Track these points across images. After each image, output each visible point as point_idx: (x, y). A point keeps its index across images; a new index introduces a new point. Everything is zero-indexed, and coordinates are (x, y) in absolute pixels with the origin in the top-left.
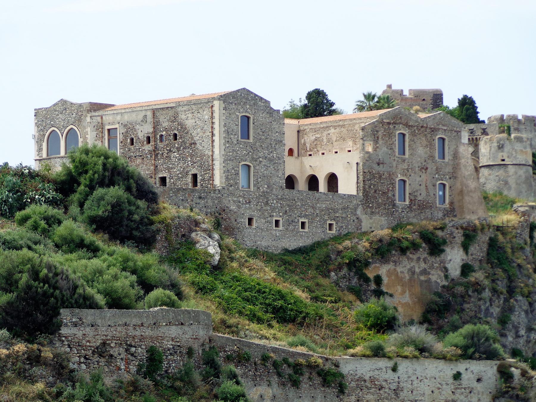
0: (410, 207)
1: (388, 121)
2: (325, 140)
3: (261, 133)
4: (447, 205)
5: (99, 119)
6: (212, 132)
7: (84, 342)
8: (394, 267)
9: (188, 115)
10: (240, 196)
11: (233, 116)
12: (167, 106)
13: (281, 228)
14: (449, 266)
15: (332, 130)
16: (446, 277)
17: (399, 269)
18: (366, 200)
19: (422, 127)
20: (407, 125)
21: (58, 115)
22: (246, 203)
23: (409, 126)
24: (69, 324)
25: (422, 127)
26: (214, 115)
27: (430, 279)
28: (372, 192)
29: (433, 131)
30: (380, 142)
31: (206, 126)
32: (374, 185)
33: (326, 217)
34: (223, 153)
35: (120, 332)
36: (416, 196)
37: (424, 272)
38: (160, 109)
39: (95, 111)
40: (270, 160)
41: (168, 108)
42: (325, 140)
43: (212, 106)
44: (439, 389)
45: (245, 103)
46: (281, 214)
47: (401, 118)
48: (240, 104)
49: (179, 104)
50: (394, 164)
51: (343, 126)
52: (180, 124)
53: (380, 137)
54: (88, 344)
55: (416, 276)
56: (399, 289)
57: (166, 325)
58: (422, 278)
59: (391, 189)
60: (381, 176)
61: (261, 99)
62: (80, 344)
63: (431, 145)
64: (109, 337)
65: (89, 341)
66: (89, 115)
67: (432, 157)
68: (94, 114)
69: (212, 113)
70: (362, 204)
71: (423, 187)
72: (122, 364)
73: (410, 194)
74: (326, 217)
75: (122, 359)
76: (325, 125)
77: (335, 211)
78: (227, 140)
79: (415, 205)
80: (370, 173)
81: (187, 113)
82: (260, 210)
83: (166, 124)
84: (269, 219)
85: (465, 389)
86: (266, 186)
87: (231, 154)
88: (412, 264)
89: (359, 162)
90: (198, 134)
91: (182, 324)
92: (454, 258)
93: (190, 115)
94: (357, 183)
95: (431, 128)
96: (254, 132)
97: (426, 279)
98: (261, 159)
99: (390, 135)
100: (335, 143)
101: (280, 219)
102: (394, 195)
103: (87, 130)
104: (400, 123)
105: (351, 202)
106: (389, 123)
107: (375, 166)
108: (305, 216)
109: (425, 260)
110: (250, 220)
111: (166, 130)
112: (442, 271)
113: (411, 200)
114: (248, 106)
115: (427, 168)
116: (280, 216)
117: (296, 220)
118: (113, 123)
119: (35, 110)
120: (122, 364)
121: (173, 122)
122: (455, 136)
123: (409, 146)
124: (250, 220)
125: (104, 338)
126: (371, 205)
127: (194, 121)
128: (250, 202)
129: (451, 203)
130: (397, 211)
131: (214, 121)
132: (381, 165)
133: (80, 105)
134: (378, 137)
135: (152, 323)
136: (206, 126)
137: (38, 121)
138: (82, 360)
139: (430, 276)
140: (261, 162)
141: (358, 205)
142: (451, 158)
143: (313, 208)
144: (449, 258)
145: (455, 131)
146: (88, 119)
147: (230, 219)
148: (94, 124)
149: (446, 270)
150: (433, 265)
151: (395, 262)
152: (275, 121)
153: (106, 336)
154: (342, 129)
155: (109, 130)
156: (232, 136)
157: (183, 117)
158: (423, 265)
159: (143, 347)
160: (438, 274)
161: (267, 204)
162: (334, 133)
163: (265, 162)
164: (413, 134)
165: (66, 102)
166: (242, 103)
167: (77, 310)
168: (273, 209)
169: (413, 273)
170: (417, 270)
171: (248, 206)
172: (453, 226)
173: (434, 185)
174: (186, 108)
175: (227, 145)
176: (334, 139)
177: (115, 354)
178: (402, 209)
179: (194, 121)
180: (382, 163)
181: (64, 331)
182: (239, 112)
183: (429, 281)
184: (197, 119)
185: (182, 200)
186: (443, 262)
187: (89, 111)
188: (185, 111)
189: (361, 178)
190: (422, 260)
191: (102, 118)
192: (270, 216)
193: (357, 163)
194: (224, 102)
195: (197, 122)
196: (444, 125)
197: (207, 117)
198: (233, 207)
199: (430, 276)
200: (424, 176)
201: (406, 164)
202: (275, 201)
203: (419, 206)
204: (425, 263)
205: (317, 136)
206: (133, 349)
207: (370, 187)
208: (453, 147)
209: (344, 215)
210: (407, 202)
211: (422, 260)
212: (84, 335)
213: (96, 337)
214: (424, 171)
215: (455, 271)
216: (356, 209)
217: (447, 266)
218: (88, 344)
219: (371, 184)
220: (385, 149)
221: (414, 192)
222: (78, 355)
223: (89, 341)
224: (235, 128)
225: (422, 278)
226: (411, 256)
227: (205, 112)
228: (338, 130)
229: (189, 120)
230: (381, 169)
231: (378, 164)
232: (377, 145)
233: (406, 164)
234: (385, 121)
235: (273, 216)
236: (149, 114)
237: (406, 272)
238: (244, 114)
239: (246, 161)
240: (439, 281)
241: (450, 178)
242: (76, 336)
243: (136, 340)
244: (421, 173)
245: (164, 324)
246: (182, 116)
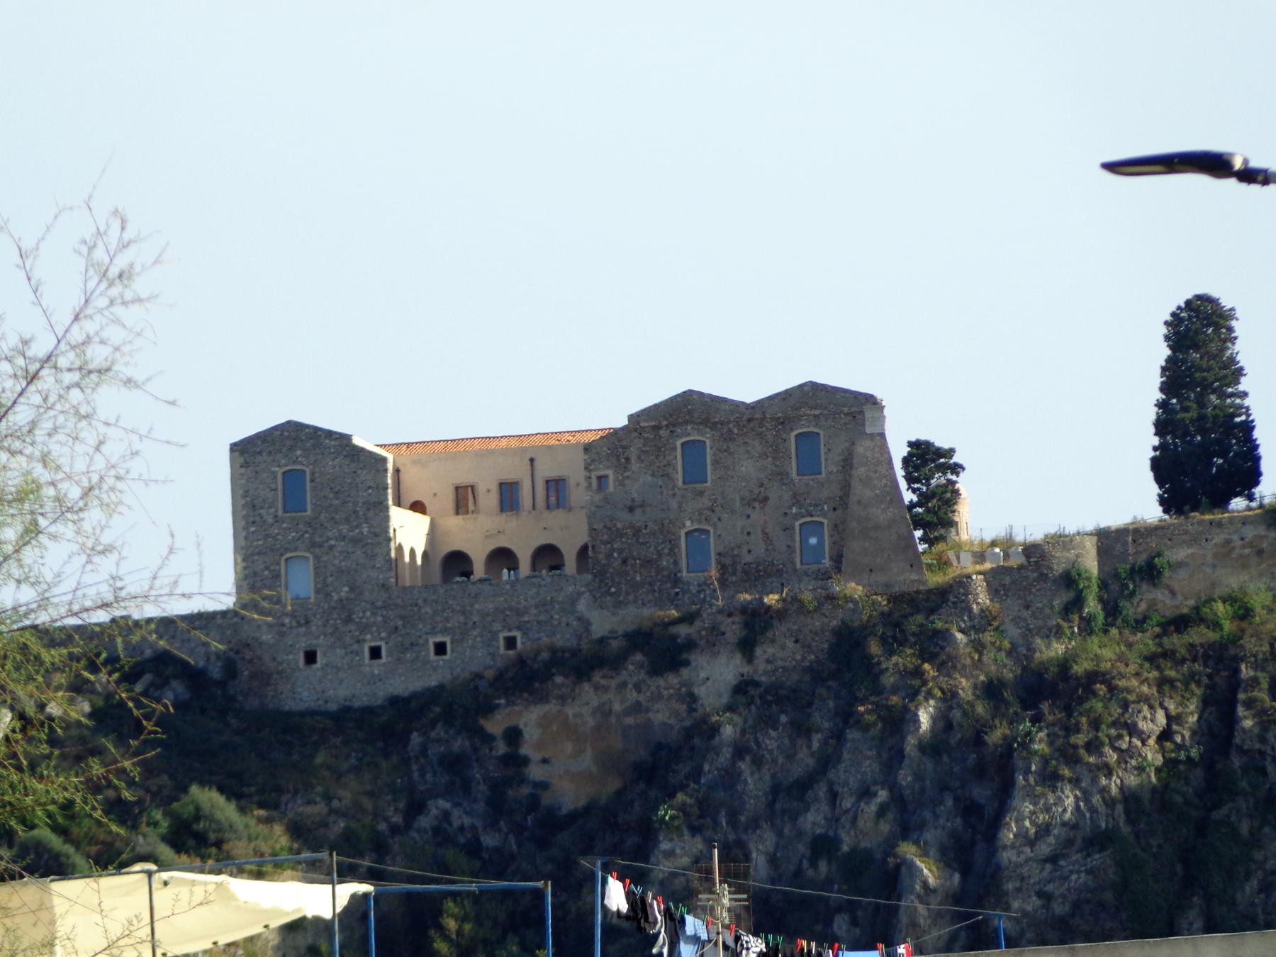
3: (331, 495)
8: (558, 707)
11: (265, 475)
13: (384, 659)
14: (700, 691)
16: (691, 710)
17: (570, 712)
18: (601, 581)
22: (300, 625)
23: (715, 423)
27: (650, 720)
28: (616, 564)
30: (635, 466)
32: (620, 551)
33: (497, 626)
34: (243, 543)
40: (355, 541)
45: (291, 449)
46: (383, 635)
50: (674, 504)
56: (569, 747)
58: (629, 721)
61: (330, 434)
67: (782, 476)
74: (497, 626)
77: (519, 613)
78: (251, 519)
79: (734, 574)
82: (332, 634)
84: (355, 647)
86: (346, 589)
87: (260, 542)
98: (332, 542)
102: (676, 563)
107: (625, 516)
108: (445, 631)
109: (638, 688)
110: (311, 657)
114: (299, 452)
115: (766, 499)
116: (382, 639)
117: (421, 641)
122: (845, 424)
124: (311, 657)
126: (613, 590)
128: (307, 622)
130: (688, 591)
132: (638, 511)
134: (627, 459)
139: (650, 715)
140: (331, 547)
141: (580, 594)
143: (463, 613)
144: (703, 675)
147: (260, 658)
158: (632, 695)
161: (348, 620)
163: (341, 545)
166: (284, 450)
168: (364, 628)
170: (617, 707)
171: (303, 630)
175: (253, 529)
180: (641, 506)
186: (688, 684)
192: (358, 642)
196: (811, 408)
198: (267, 637)
199: (650, 715)
202: (368, 614)
203: (745, 572)
204: (639, 691)
209: (542, 618)
211: (630, 686)
216: (573, 601)
217: (696, 690)
225: (629, 721)
226: (603, 682)
230: (638, 518)
231: (631, 509)
234: (643, 424)
235: (364, 641)
239: (296, 549)
244: (749, 511)
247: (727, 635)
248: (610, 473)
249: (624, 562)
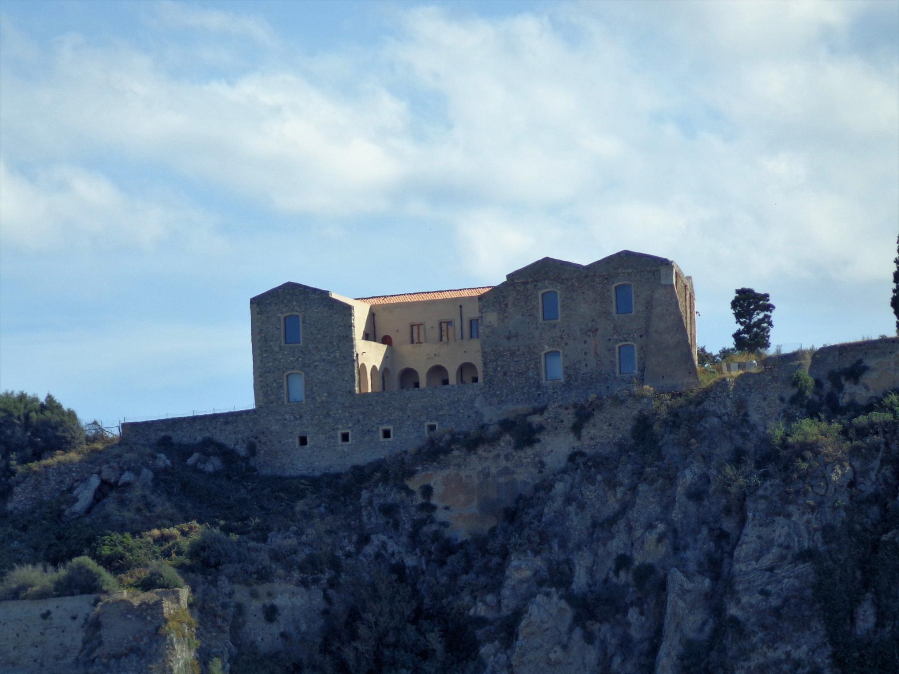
10: (286, 413)
17: (463, 473)
19: (586, 276)
22: (296, 419)
28: (499, 375)
30: (511, 309)
32: (503, 367)
44: (25, 631)
46: (350, 425)
58: (502, 480)
61: (315, 290)
74: (423, 418)
84: (332, 433)
85: (57, 628)
86: (326, 394)
101: (349, 431)
102: (538, 375)
106: (526, 283)
108: (389, 422)
114: (294, 303)
116: (349, 428)
117: (374, 429)
128: (301, 417)
134: (506, 305)
139: (515, 476)
140: (316, 367)
144: (549, 448)
151: (459, 466)
158: (503, 463)
161: (328, 415)
170: (493, 471)
171: (298, 422)
185: (201, 430)
198: (275, 428)
199: (515, 476)
202: (340, 411)
207: (495, 370)
209: (452, 412)
211: (502, 457)
217: (545, 460)
225: (502, 480)
226: (484, 454)
231: (509, 338)
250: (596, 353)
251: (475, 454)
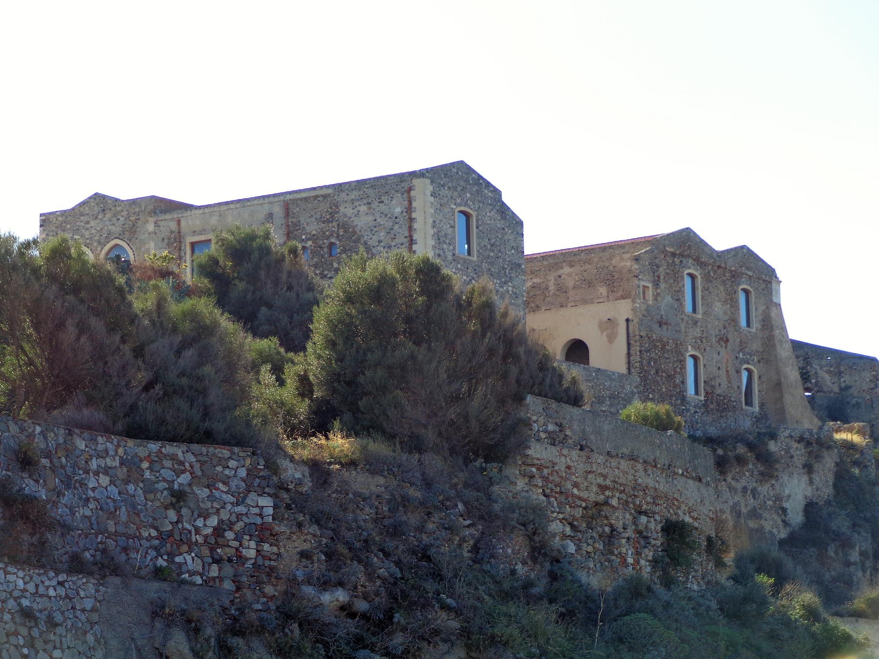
0: (705, 405)
1: (672, 250)
2: (552, 288)
3: (489, 247)
4: (756, 409)
5: (173, 226)
6: (411, 236)
7: (569, 485)
9: (359, 208)
11: (446, 210)
12: (314, 193)
15: (567, 270)
16: (786, 523)
18: (645, 386)
19: (719, 267)
20: (698, 261)
21: (88, 222)
23: (702, 263)
24: (543, 435)
25: (719, 267)
26: (414, 204)
28: (652, 373)
29: (734, 276)
30: (663, 285)
31: (396, 227)
35: (622, 471)
36: (713, 387)
37: (754, 514)
38: (301, 199)
39: (164, 212)
41: (317, 196)
42: (552, 288)
43: (410, 189)
45: (464, 189)
47: (689, 247)
48: (455, 188)
49: (339, 188)
51: (589, 261)
52: (344, 226)
53: (662, 277)
54: (575, 491)
55: (742, 520)
57: (683, 474)
58: (752, 524)
59: (678, 370)
60: (664, 346)
61: (488, 184)
62: (563, 490)
63: (732, 301)
64: (608, 482)
65: (576, 485)
66: (152, 220)
67: (734, 321)
68: (163, 217)
69: (410, 203)
70: (639, 393)
71: (723, 373)
72: (630, 552)
73: (705, 382)
75: (628, 539)
76: (551, 261)
78: (437, 252)
79: (712, 403)
80: (649, 338)
81: (356, 204)
83: (313, 228)
88: (737, 498)
89: (631, 317)
90: (380, 242)
91: (700, 480)
92: (796, 490)
93: (363, 208)
94: (629, 354)
95: (731, 271)
96: (479, 244)
97: (756, 526)
99: (676, 276)
100: (571, 293)
102: (683, 382)
103: (147, 246)
104: (689, 256)
105: (623, 387)
106: (673, 255)
107: (656, 327)
111: (313, 238)
112: (778, 514)
113: (707, 393)
114: (468, 195)
118: (203, 232)
119: (41, 215)
120: (630, 552)
121: (328, 221)
122: (763, 290)
123: (703, 297)
125: (600, 480)
126: (651, 396)
127: (371, 218)
129: (762, 405)
130: (688, 410)
131: (414, 215)
132: (665, 327)
133: (134, 202)
134: (659, 277)
135: (667, 463)
136: (396, 227)
137: (47, 235)
138: (568, 530)
139: (763, 522)
141: (633, 393)
142: (760, 327)
144: (787, 492)
145: (764, 281)
146: (151, 227)
148: (163, 235)
149: (784, 510)
150: (765, 502)
152: (509, 227)
153: (605, 477)
154: (587, 266)
155: (193, 245)
156: (445, 246)
157: (349, 211)
159: (658, 518)
160: (773, 519)
162: (570, 275)
164: (707, 278)
165: (104, 197)
166: (459, 189)
167: (554, 405)
169: (739, 514)
170: (744, 510)
172: (791, 437)
173: (738, 372)
174: (354, 195)
176: (570, 283)
177: (619, 525)
178: (695, 407)
179: (371, 218)
180: (666, 324)
181: (538, 451)
182: (455, 204)
183: (760, 530)
184: (378, 215)
186: (778, 498)
187: (154, 212)
188: (353, 200)
189: (636, 349)
190: (749, 492)
191: (179, 222)
193: (627, 320)
194: (432, 182)
195: (379, 220)
196: (748, 269)
197: (398, 210)
199: (763, 522)
200: (723, 352)
201: (698, 330)
204: (754, 497)
205: (535, 280)
206: (644, 519)
207: (649, 363)
208: (762, 308)
209: (613, 410)
210: (702, 398)
211: (749, 492)
212: (569, 467)
213: (590, 476)
214: (723, 343)
215: (797, 517)
217: (785, 505)
218: (575, 491)
219: (651, 358)
220: (668, 299)
221: (711, 379)
222: (561, 516)
223: (576, 485)
224: (450, 231)
225: (752, 524)
226: (733, 483)
227: (394, 202)
228: (577, 268)
229: (362, 219)
231: (660, 324)
232: (659, 291)
233: (698, 330)
234: (668, 249)
236: (278, 211)
237: (728, 511)
238: (463, 208)
240: (775, 531)
241: (759, 361)
242: (556, 468)
243: (649, 499)
244: (719, 348)
245: (680, 471)
246: (346, 210)
247: (796, 459)
248: (650, 285)
249: (657, 372)
250: (727, 371)
251: (725, 480)
